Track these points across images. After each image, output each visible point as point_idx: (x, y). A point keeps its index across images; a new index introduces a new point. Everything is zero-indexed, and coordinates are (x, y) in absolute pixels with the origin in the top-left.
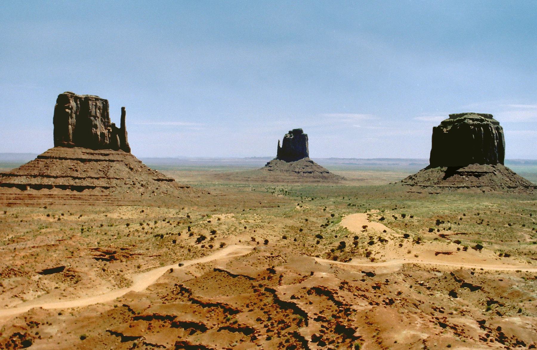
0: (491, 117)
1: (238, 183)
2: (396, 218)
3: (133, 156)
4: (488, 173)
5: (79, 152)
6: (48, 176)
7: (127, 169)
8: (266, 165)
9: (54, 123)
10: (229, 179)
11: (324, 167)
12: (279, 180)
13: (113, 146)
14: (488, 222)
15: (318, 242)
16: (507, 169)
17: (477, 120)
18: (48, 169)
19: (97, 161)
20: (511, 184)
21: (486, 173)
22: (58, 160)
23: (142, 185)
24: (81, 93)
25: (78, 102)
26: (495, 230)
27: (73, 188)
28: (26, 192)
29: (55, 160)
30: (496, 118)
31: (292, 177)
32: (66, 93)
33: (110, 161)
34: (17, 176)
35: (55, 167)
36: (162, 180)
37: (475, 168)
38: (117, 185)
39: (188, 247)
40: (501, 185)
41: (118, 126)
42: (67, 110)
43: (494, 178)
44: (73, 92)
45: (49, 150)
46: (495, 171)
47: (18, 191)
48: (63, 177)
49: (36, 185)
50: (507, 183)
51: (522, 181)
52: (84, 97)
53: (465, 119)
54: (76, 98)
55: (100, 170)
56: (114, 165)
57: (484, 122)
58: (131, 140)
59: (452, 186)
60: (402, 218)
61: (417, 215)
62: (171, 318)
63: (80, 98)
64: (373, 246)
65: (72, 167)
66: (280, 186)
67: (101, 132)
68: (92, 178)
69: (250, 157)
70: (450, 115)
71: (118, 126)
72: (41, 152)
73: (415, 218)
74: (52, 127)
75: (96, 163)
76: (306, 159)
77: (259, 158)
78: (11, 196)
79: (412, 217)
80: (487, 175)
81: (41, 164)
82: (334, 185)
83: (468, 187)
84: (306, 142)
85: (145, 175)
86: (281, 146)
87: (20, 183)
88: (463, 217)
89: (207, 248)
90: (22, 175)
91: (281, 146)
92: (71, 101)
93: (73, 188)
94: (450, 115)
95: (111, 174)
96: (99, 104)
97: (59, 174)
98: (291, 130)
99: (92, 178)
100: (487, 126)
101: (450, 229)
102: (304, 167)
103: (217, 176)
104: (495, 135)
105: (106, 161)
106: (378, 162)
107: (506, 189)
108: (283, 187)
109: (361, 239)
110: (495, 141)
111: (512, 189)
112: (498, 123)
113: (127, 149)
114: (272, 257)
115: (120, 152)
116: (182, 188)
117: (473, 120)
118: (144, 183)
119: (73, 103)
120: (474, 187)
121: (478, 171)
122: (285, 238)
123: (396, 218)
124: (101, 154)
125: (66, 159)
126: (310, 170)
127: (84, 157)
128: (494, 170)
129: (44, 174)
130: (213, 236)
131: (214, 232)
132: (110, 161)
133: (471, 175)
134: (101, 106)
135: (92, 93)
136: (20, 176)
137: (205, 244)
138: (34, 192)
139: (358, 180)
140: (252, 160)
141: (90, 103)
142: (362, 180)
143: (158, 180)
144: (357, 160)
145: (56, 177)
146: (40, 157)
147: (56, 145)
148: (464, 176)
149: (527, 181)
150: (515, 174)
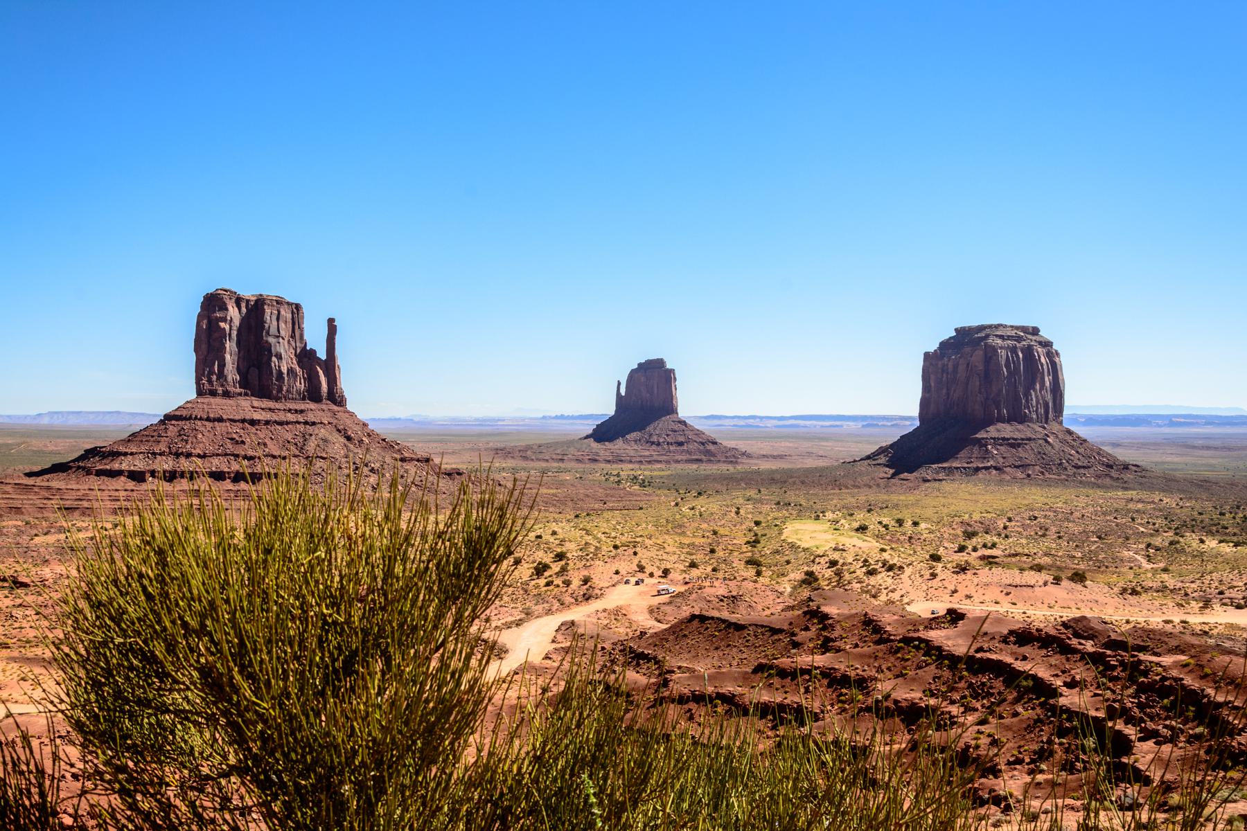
0: (1035, 331)
1: (544, 465)
2: (886, 527)
3: (352, 415)
5: (248, 406)
6: (188, 455)
7: (343, 440)
9: (196, 350)
10: (525, 458)
11: (707, 433)
13: (313, 394)
14: (1059, 533)
15: (759, 574)
16: (1070, 432)
17: (1009, 338)
18: (187, 442)
19: (281, 423)
20: (1079, 459)
21: (1030, 439)
22: (207, 423)
23: (372, 470)
24: (248, 292)
25: (244, 310)
26: (1077, 546)
27: (238, 477)
28: (144, 486)
29: (199, 423)
30: (1045, 334)
31: (647, 453)
32: (219, 292)
33: (306, 423)
34: (125, 454)
35: (200, 436)
36: (412, 459)
37: (1007, 430)
38: (323, 470)
39: (519, 584)
40: (1061, 464)
41: (322, 354)
42: (222, 325)
44: (233, 290)
45: (188, 402)
46: (1048, 436)
47: (131, 485)
48: (218, 455)
49: (165, 472)
50: (1072, 458)
51: (1099, 454)
52: (254, 299)
53: (987, 336)
54: (238, 301)
55: (289, 442)
56: (316, 432)
57: (1024, 343)
58: (347, 383)
59: (966, 465)
60: (897, 525)
61: (927, 520)
62: (728, 699)
63: (248, 301)
64: (879, 576)
65: (234, 436)
66: (626, 470)
67: (288, 370)
68: (274, 457)
69: (554, 415)
70: (956, 330)
71: (322, 354)
72: (169, 408)
73: (923, 525)
74: (193, 358)
75: (279, 427)
76: (673, 417)
77: (568, 417)
78: (117, 494)
79: (915, 524)
80: (1033, 444)
81: (172, 430)
82: (731, 467)
83: (996, 468)
84: (673, 386)
85: (378, 449)
86: (623, 394)
87: (132, 468)
88: (1008, 524)
89: (558, 586)
90: (136, 453)
91: (623, 394)
92: (230, 308)
93: (238, 477)
94: (956, 330)
95: (311, 446)
96: (286, 313)
97: (211, 449)
99: (274, 457)
100: (1028, 351)
101: (994, 545)
103: (503, 452)
104: (1045, 367)
105: (299, 423)
106: (802, 423)
107: (1071, 471)
108: (633, 472)
109: (844, 564)
110: (1046, 379)
111: (1082, 471)
112: (1047, 344)
113: (336, 398)
114: (733, 597)
115: (327, 405)
116: (449, 474)
117: (1001, 337)
118: (376, 466)
119: (233, 313)
120: (1010, 466)
121: (1015, 437)
122: (693, 565)
123: (886, 527)
124: (290, 410)
125: (220, 420)
126: (681, 439)
127: (256, 416)
128: (1046, 435)
129: (180, 451)
130: (563, 563)
131: (560, 556)
132: (306, 423)
133: (1001, 445)
134: (289, 316)
135: (270, 291)
136: (132, 454)
137: (550, 579)
138: (166, 487)
139: (774, 457)
140: (559, 421)
141: (268, 310)
142: (781, 457)
143: (403, 460)
144: (761, 418)
145: (203, 456)
146: (168, 417)
147: (200, 393)
149: (1110, 455)
150: (1085, 441)
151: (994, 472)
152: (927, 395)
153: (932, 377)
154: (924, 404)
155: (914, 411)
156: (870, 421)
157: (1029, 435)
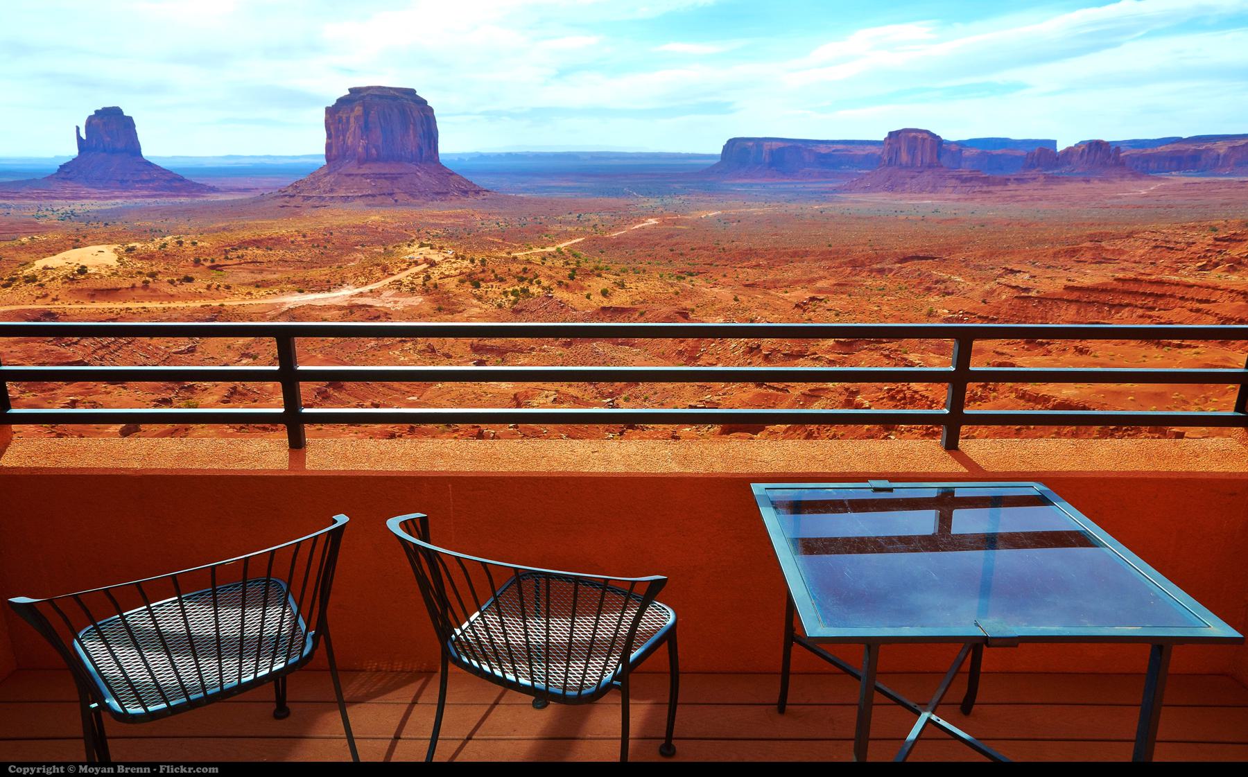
4: (407, 174)
8: (59, 170)
11: (174, 172)
12: (81, 195)
43: (417, 181)
46: (419, 171)
70: (349, 90)
83: (373, 196)
91: (83, 135)
94: (350, 90)
98: (100, 108)
102: (135, 172)
120: (384, 194)
121: (391, 172)
133: (378, 178)
148: (368, 181)
151: (371, 198)
152: (330, 141)
153: (332, 127)
154: (329, 147)
155: (322, 151)
156: (57, 158)
157: (403, 171)
